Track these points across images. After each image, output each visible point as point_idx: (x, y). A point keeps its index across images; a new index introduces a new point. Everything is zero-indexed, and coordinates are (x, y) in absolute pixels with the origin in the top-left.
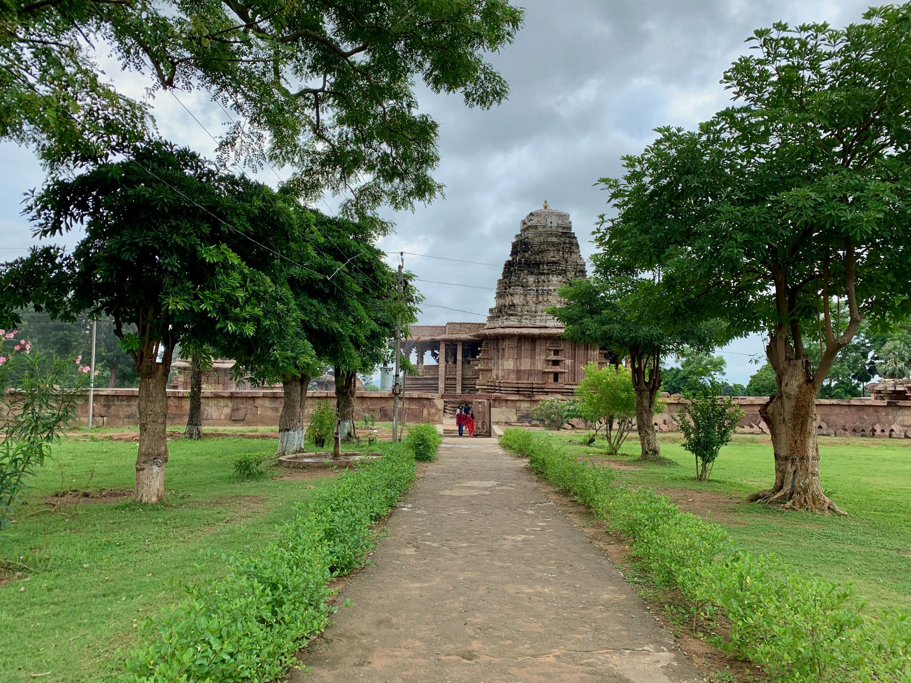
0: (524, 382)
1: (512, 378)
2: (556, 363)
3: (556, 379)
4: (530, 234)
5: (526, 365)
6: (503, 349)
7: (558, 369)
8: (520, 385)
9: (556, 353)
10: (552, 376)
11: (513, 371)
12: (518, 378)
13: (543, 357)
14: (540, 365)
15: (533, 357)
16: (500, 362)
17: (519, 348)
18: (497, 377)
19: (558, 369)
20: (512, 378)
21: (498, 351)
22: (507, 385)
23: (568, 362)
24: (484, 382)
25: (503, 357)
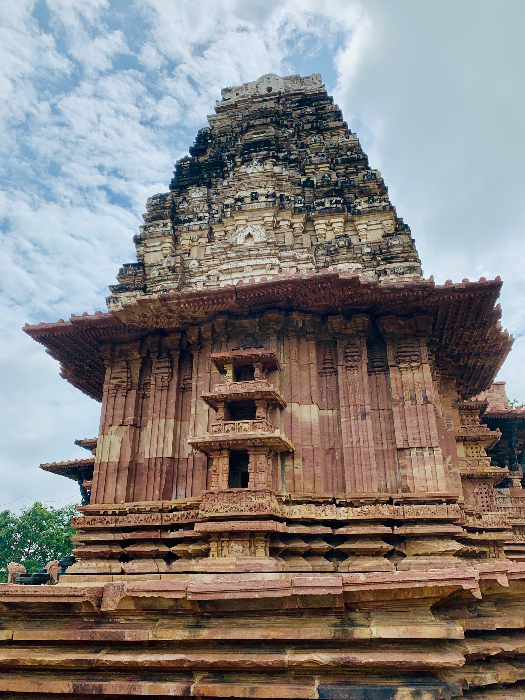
2: (238, 409)
9: (243, 372)
15: (181, 414)
23: (307, 413)
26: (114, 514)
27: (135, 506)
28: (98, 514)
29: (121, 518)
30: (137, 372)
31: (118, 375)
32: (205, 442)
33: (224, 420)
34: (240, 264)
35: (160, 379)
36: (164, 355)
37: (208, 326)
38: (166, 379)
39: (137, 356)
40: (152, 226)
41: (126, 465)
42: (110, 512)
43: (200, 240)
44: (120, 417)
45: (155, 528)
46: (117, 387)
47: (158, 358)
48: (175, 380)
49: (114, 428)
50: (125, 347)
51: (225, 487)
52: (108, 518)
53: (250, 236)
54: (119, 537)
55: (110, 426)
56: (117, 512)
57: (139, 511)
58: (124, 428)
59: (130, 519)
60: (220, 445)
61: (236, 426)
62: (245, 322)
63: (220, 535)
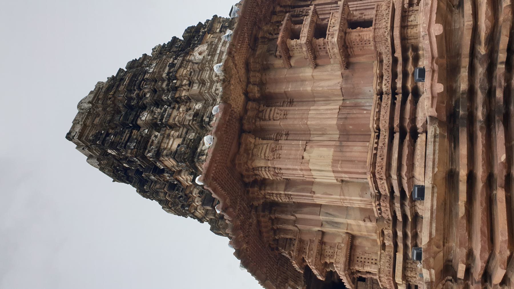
0: (372, 112)
1: (360, 151)
3: (367, 24)
4: (91, 134)
5: (324, 116)
6: (289, 183)
7: (335, 25)
8: (384, 125)
10: (355, 34)
11: (340, 148)
12: (363, 135)
13: (308, 72)
14: (328, 78)
16: (320, 199)
17: (279, 135)
18: (366, 214)
19: (335, 25)
20: (360, 151)
21: (300, 206)
22: (381, 162)
24: (385, 265)
25: (308, 185)
26: (377, 143)
27: (374, 120)
28: (375, 155)
29: (381, 137)
30: (265, 142)
31: (263, 152)
32: (340, 30)
33: (325, 38)
34: (218, 52)
35: (277, 115)
36: (260, 115)
37: (252, 74)
38: (279, 112)
39: (253, 141)
40: (151, 145)
41: (338, 143)
42: (376, 145)
43: (181, 109)
44: (298, 150)
45: (393, 104)
46: (273, 151)
47: (261, 119)
48: (281, 108)
49: (305, 155)
50: (242, 150)
51: (371, 28)
52: (380, 144)
53: (200, 54)
54: (397, 136)
55: (303, 158)
56: (376, 140)
57: (378, 119)
58: (308, 148)
59: (383, 122)
60: (343, 31)
61: (332, 25)
62: (258, 53)
63: (404, 26)
